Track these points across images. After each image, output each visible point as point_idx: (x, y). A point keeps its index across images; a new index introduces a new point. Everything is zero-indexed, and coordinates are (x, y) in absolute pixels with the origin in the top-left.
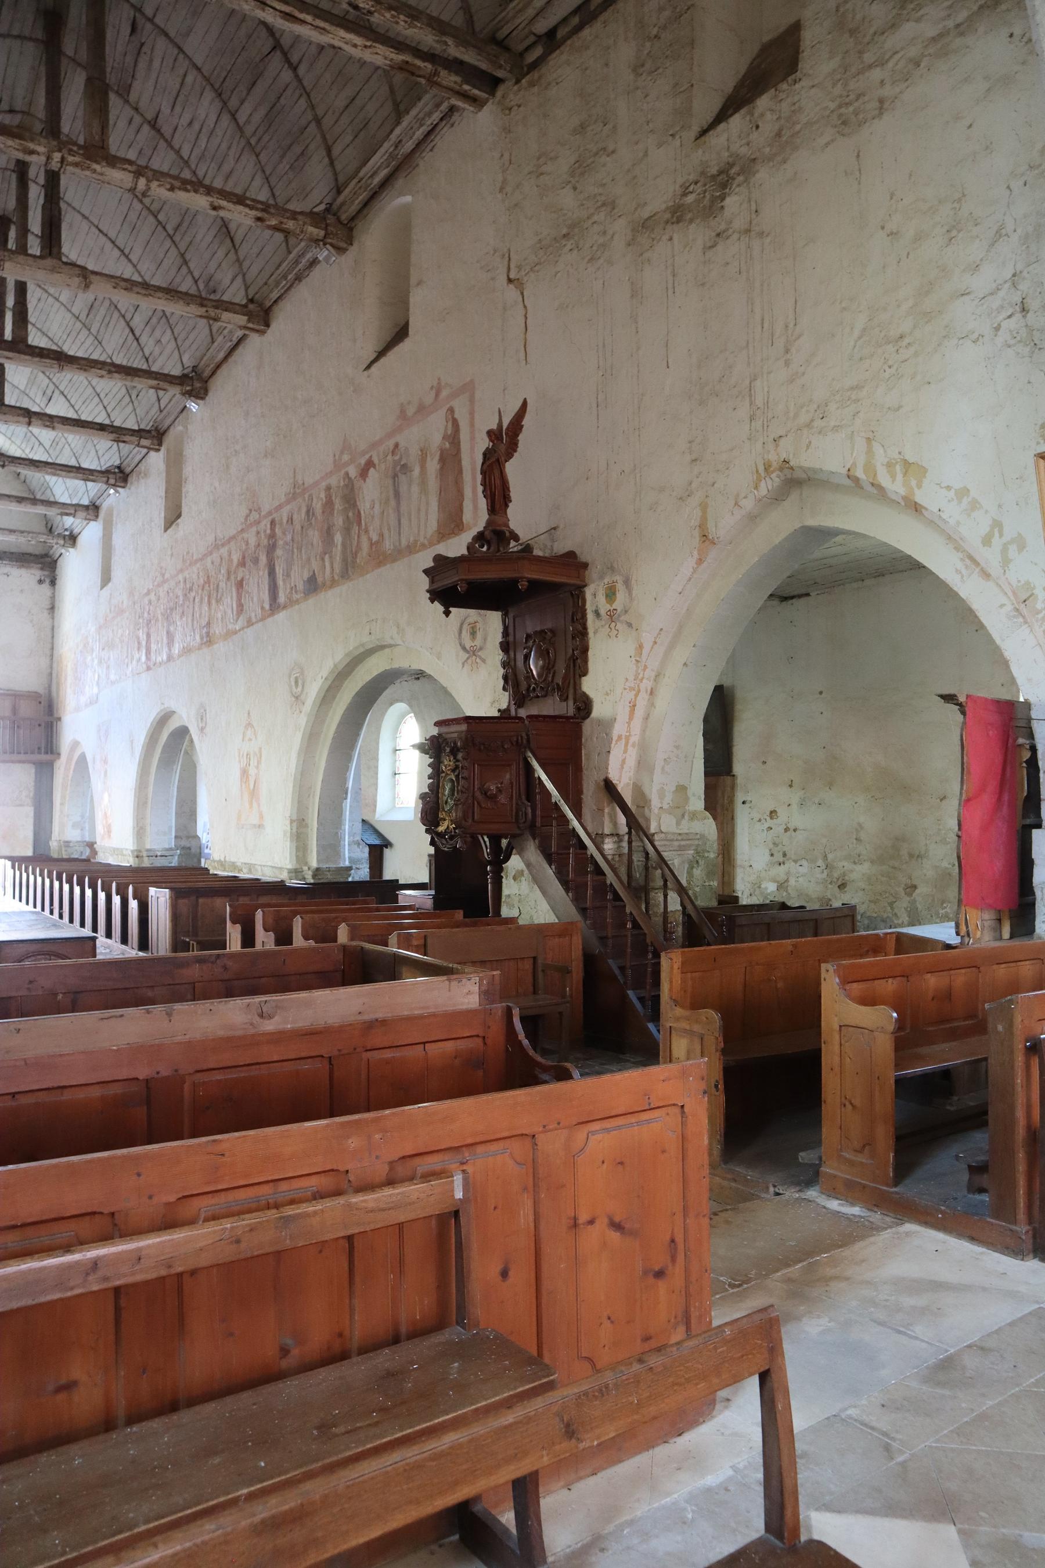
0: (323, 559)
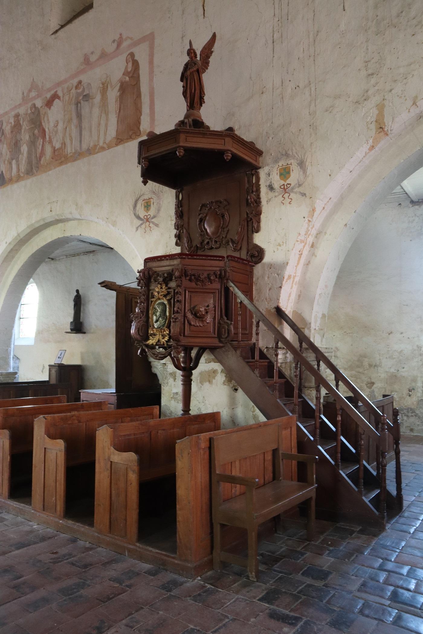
0: (10, 163)
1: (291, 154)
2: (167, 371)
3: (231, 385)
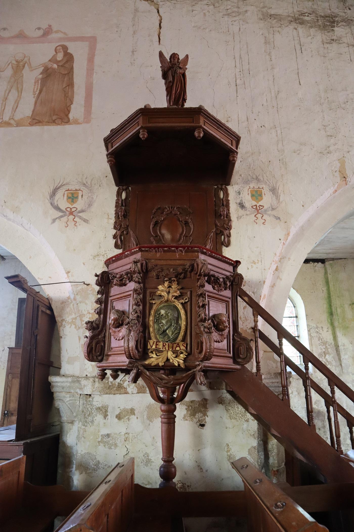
1: (262, 179)
2: (92, 405)
3: (195, 420)
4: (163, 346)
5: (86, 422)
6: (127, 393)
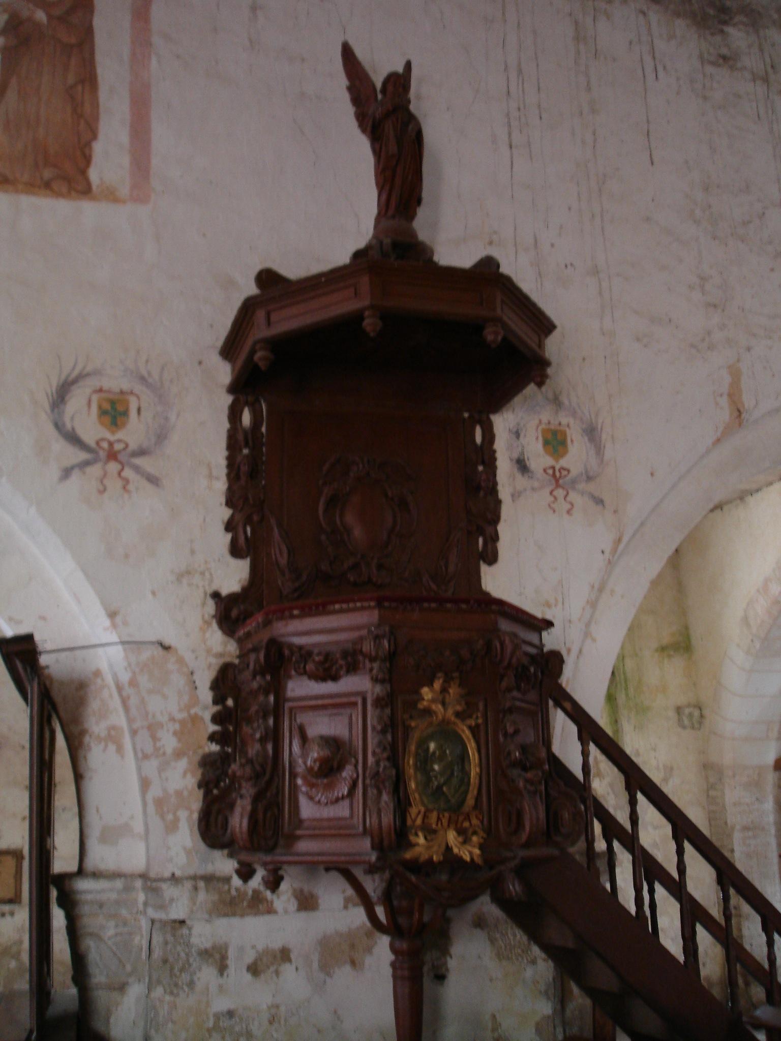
4: (439, 819)
5: (176, 985)
6: (271, 911)
